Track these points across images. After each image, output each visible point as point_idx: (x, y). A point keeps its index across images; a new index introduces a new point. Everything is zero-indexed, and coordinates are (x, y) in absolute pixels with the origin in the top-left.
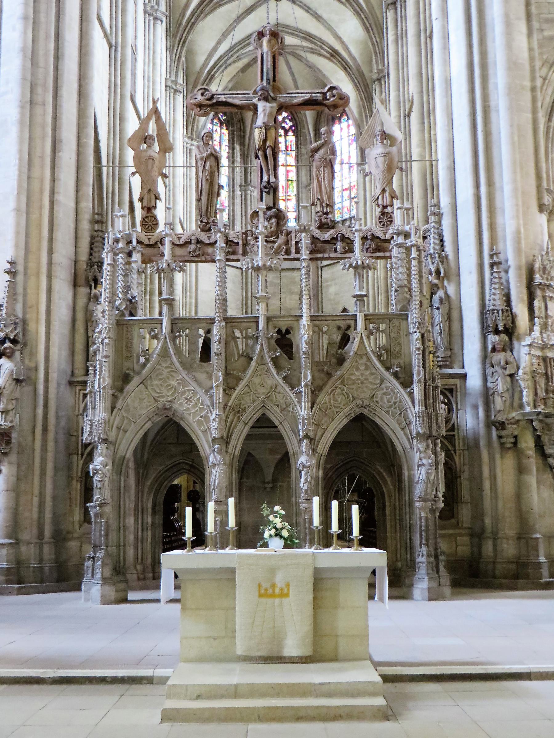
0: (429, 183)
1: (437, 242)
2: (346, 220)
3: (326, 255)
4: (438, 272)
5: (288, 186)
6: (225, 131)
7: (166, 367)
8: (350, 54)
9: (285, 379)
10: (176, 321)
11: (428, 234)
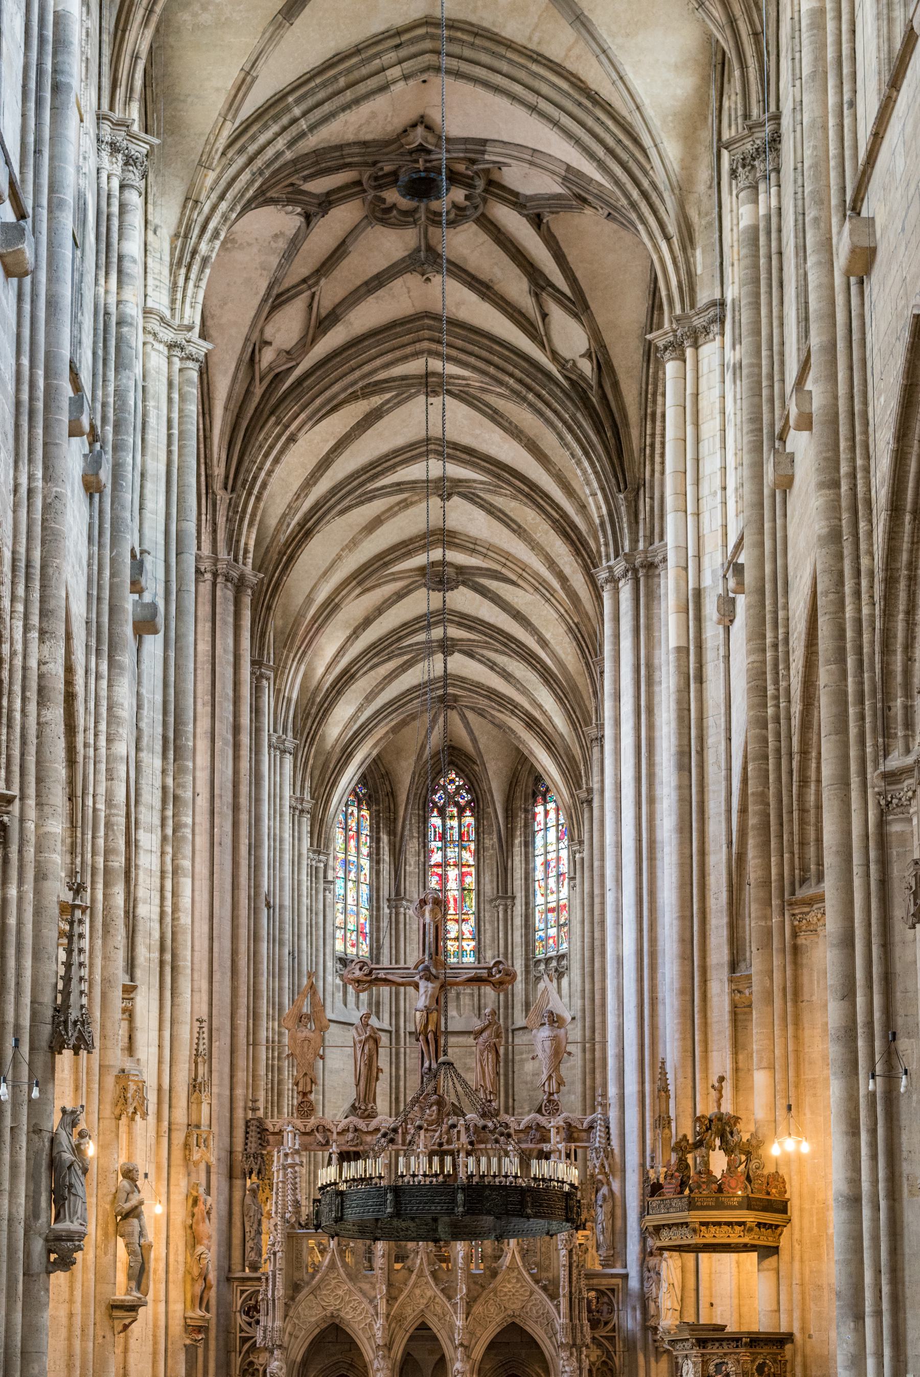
2: (551, 958)
5: (463, 899)
9: (442, 1290)
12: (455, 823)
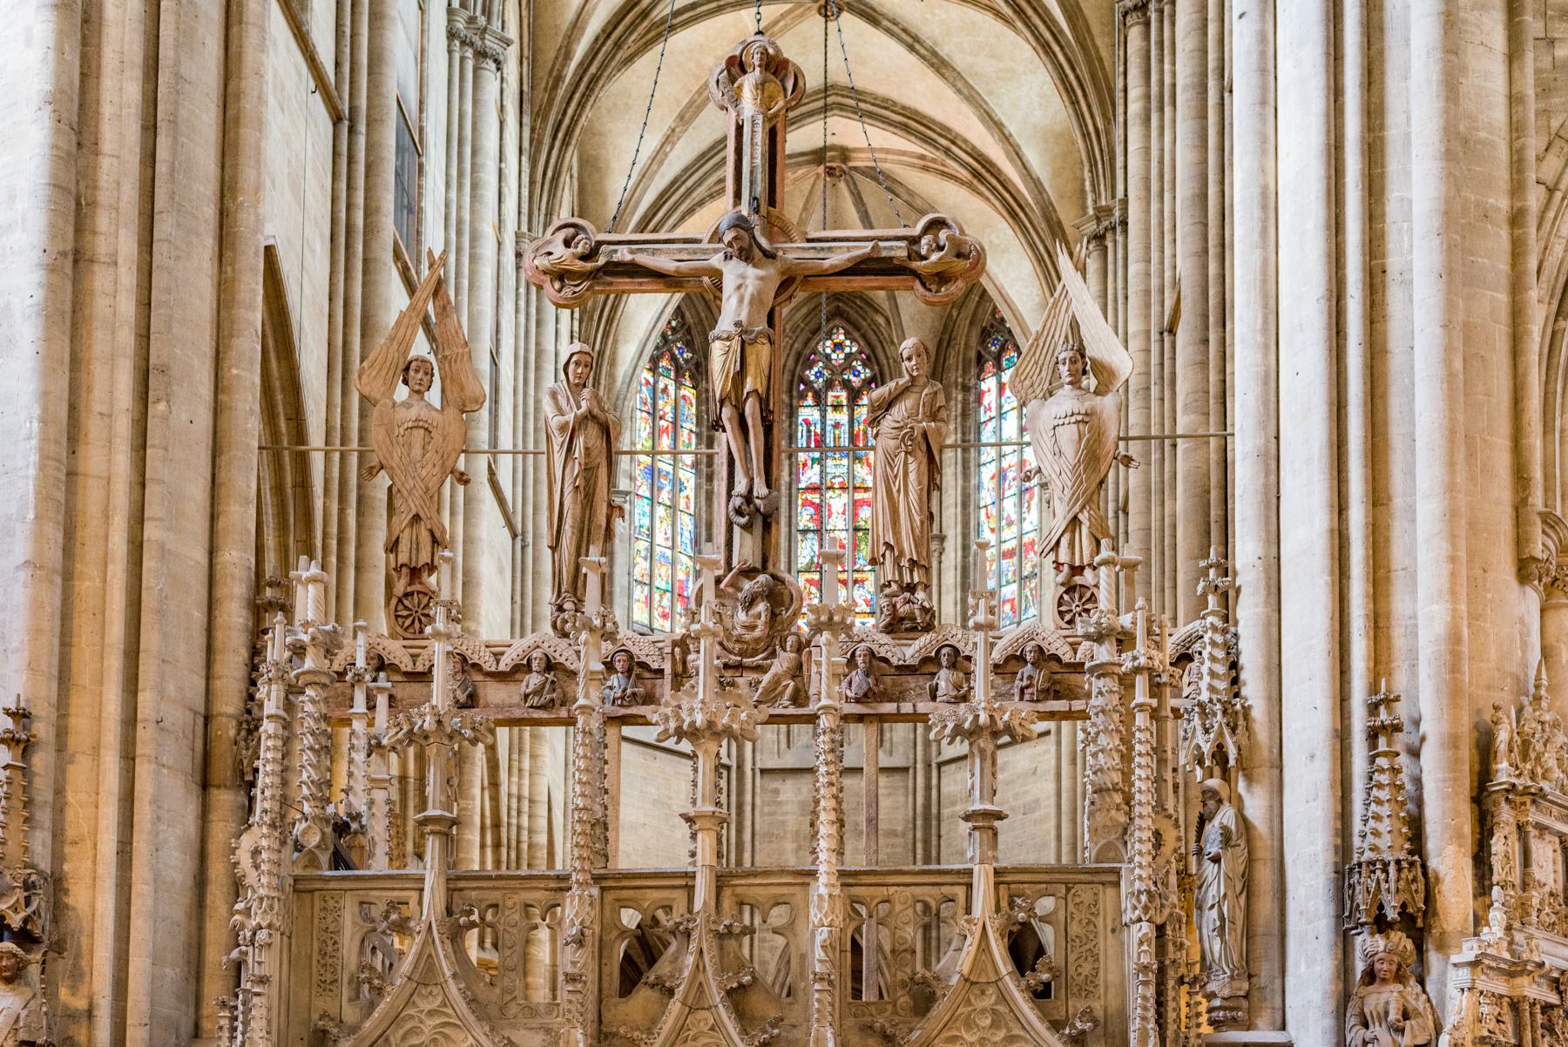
0: (1215, 512)
1: (1221, 669)
3: (907, 708)
4: (1220, 754)
6: (689, 392)
7: (431, 1013)
8: (1025, 167)
10: (462, 884)
11: (1197, 647)
12: (843, 417)
